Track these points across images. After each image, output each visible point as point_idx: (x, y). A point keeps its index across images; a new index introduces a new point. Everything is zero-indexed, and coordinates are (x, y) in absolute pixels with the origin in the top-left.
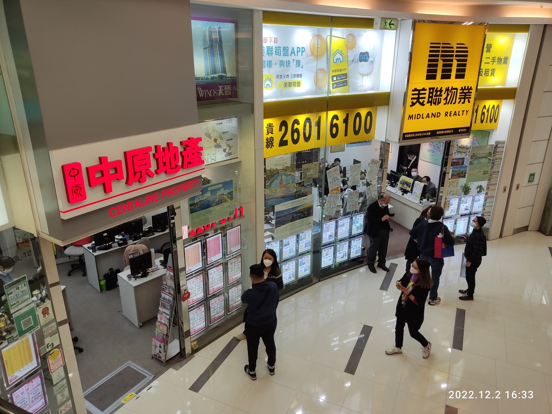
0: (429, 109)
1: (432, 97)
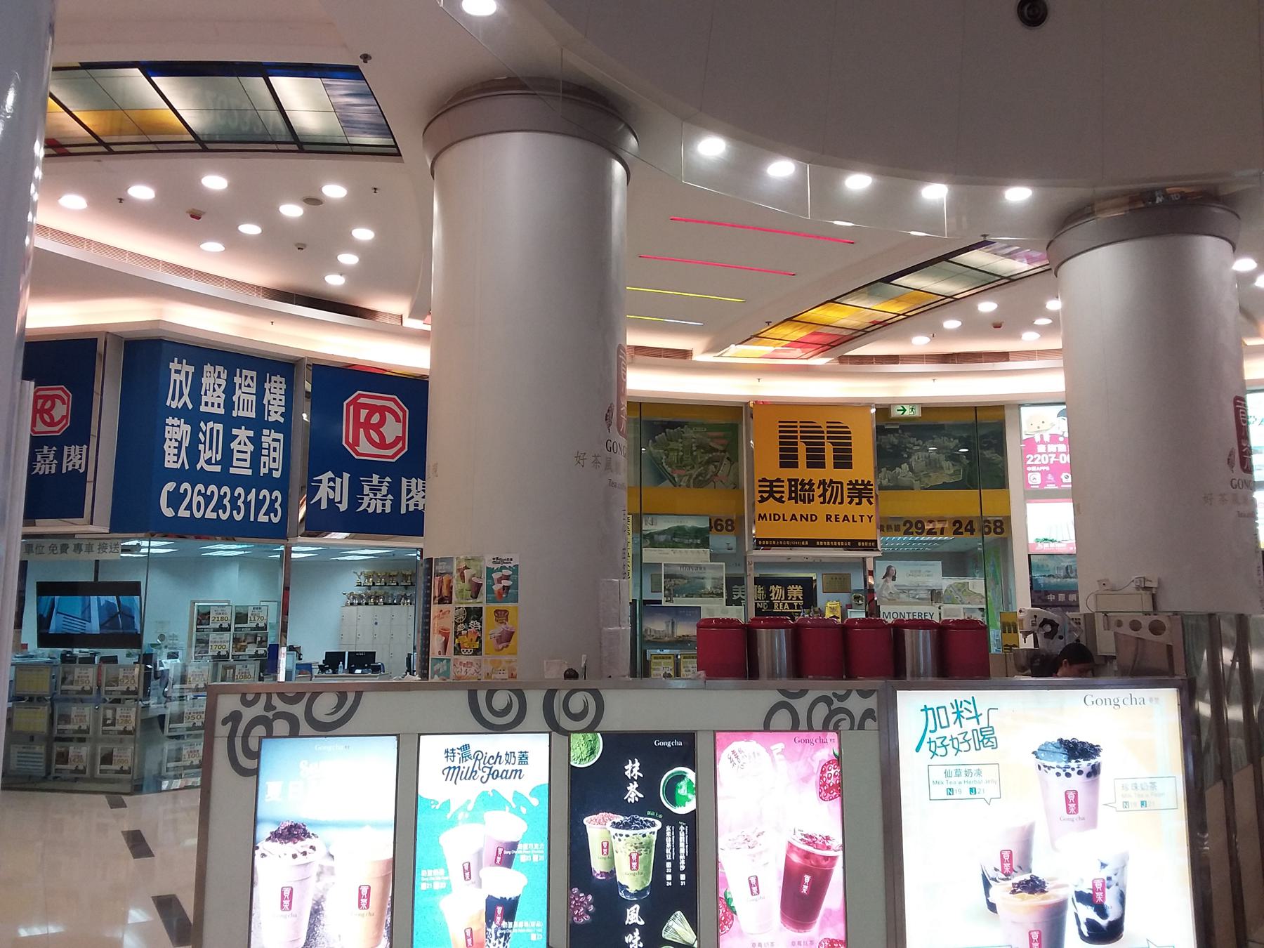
0: (790, 507)
1: (796, 492)
